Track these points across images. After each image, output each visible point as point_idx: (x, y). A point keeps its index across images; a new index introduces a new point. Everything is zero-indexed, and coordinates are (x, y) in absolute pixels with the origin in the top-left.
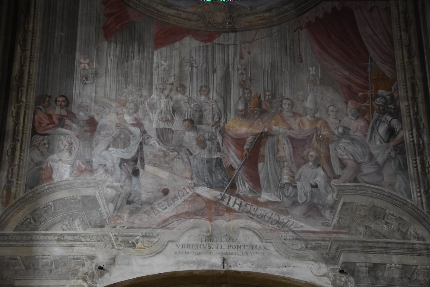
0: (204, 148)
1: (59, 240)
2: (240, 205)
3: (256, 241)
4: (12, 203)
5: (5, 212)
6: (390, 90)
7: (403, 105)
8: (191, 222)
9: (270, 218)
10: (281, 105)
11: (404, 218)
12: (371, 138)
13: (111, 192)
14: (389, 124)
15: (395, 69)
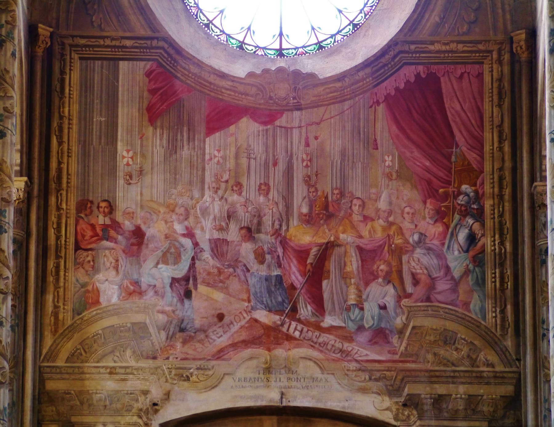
0: (262, 262)
1: (111, 373)
2: (301, 332)
3: (317, 373)
4: (61, 331)
5: (55, 341)
6: (475, 185)
7: (488, 204)
8: (248, 352)
9: (333, 346)
10: (351, 207)
11: (475, 342)
12: (449, 247)
13: (162, 318)
14: (471, 229)
15: (482, 157)
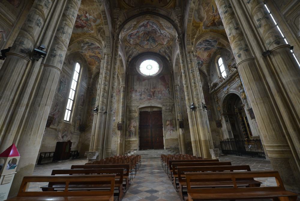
3: (154, 103)
8: (147, 101)
13: (139, 98)
